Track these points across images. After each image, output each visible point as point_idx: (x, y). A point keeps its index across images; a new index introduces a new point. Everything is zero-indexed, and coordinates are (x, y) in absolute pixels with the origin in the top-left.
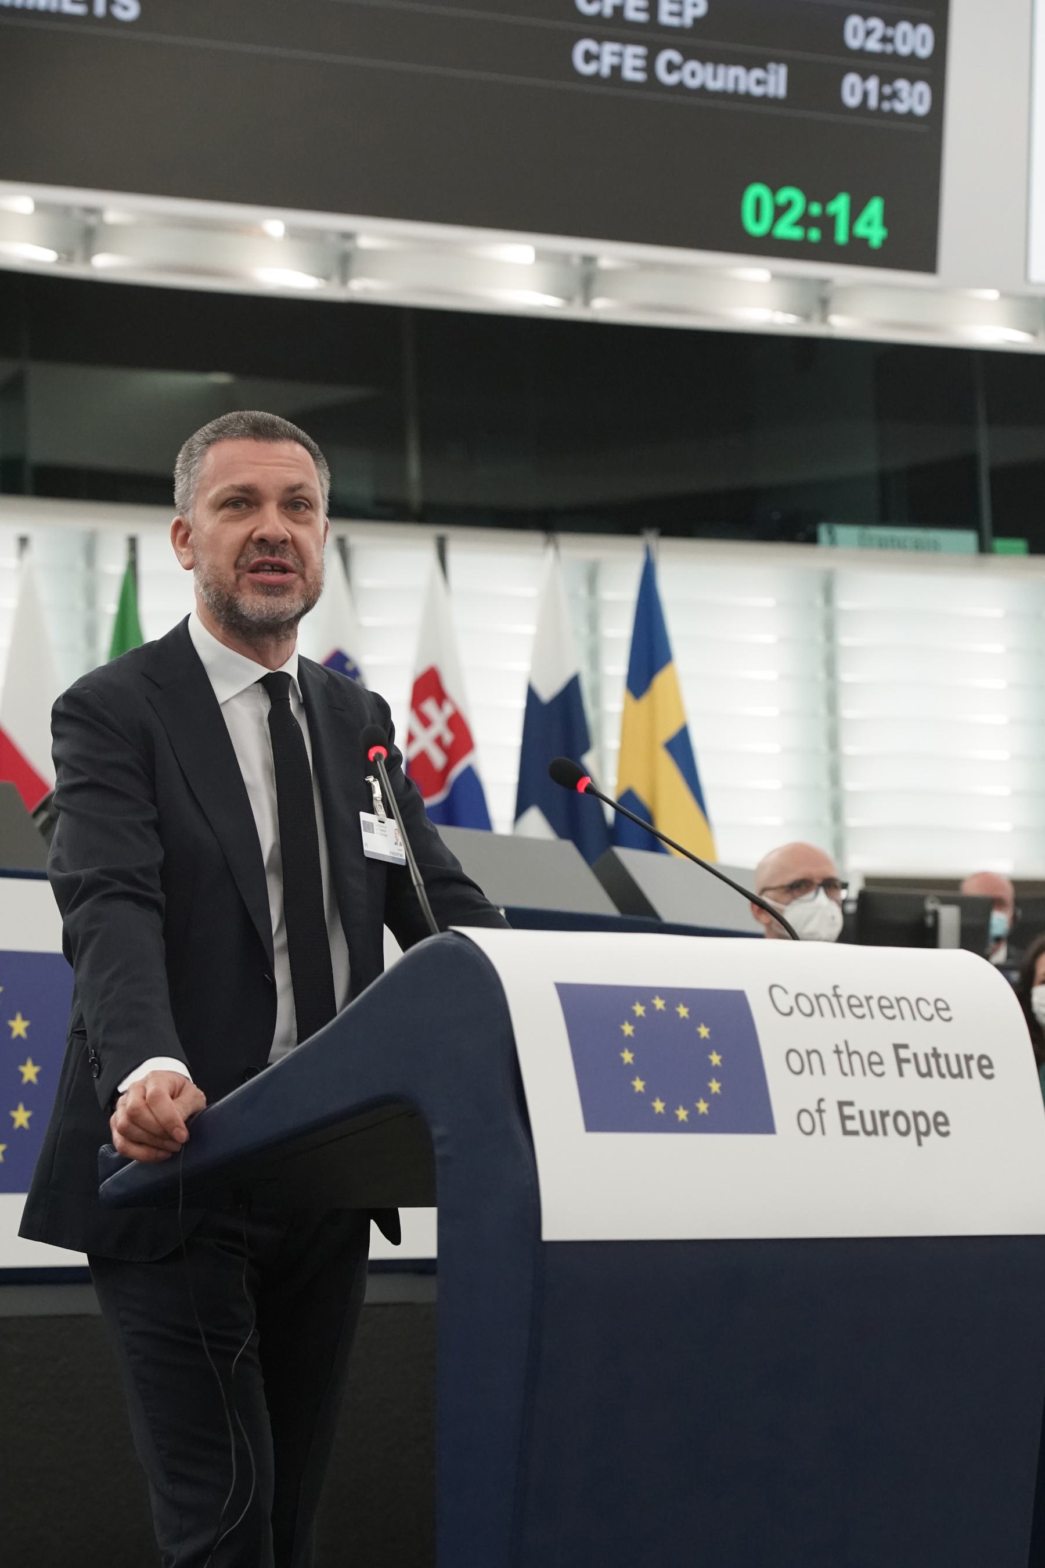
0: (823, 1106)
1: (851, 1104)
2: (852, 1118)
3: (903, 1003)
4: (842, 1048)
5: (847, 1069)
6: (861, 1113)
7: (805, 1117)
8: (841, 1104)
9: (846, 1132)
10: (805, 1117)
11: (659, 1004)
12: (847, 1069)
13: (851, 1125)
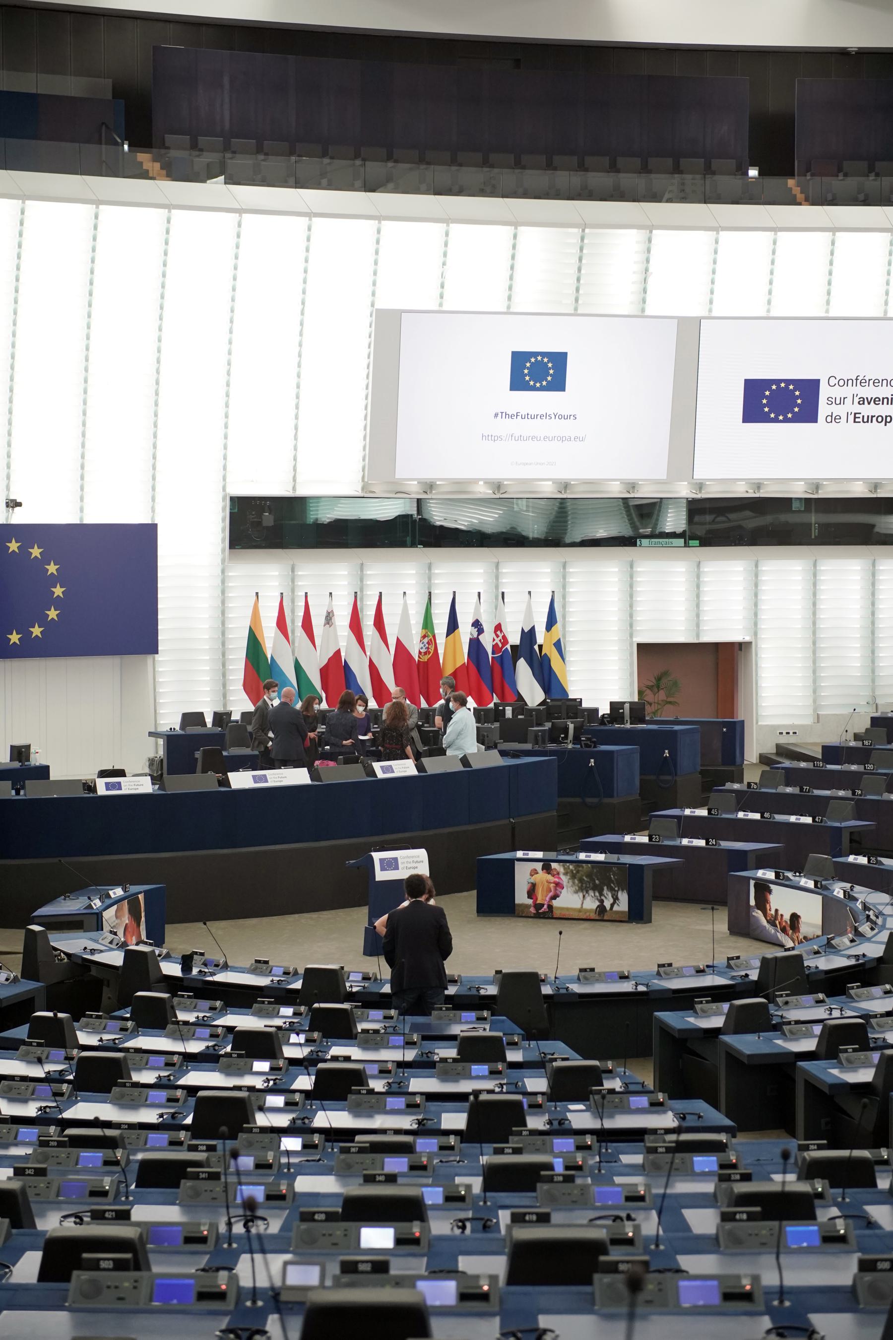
3: (885, 382)
9: (855, 422)
13: (857, 420)
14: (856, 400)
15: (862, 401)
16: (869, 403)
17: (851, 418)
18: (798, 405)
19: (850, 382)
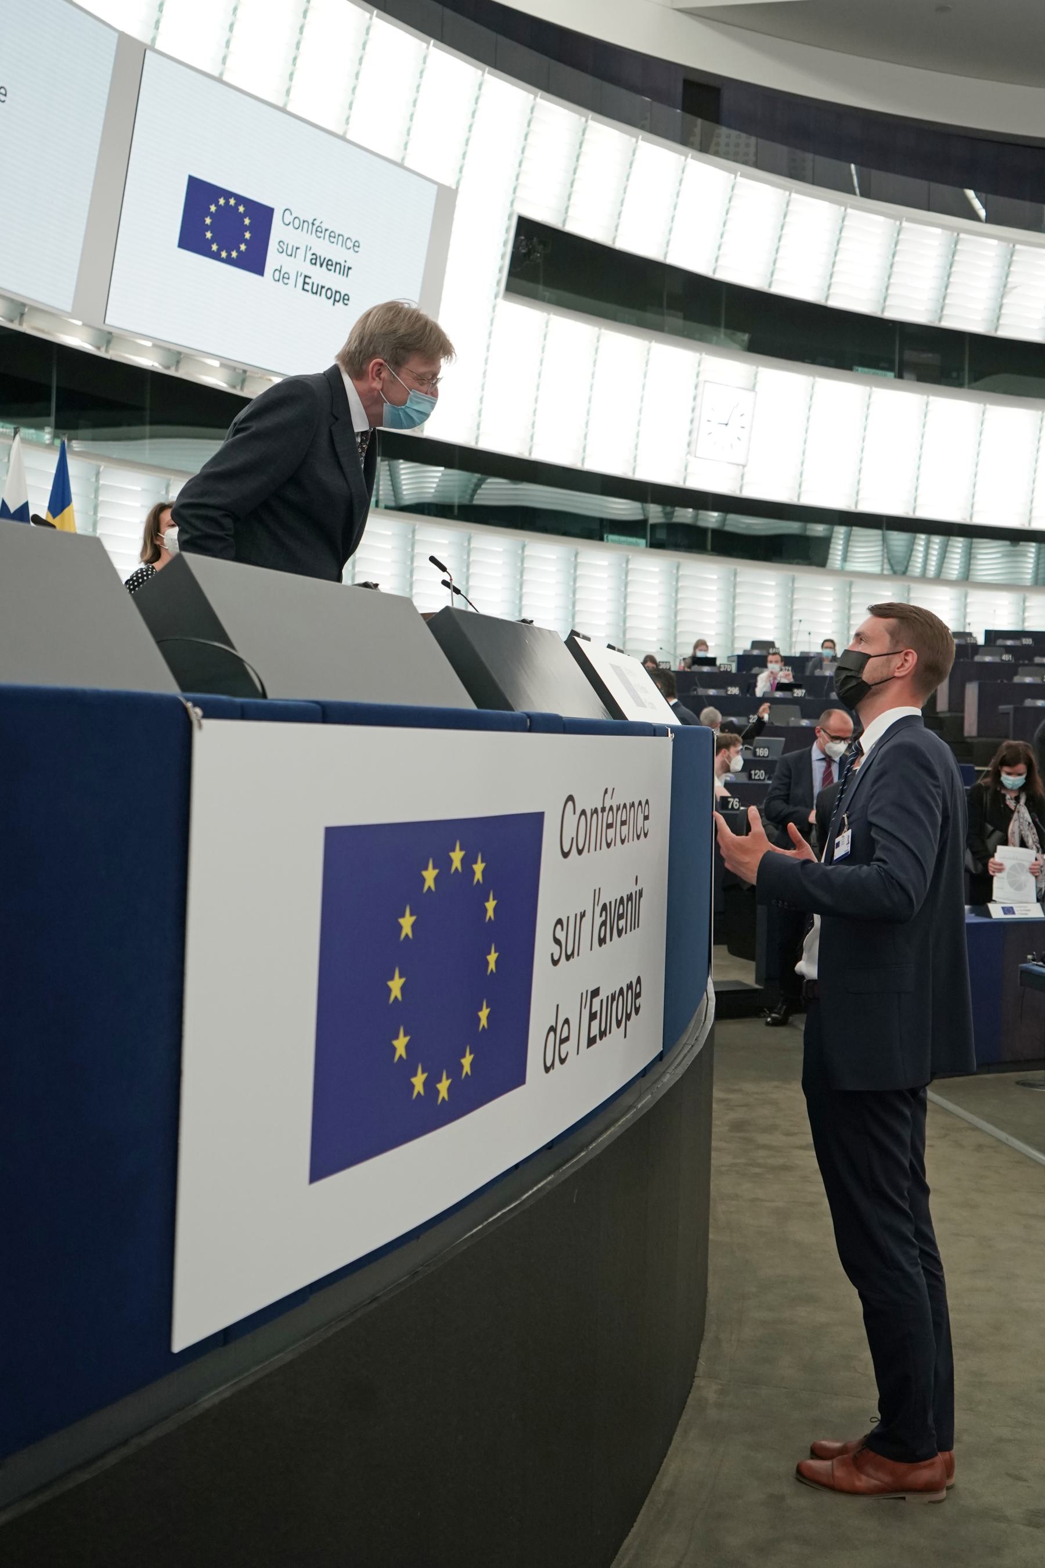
8: (306, 276)
11: (232, 202)
13: (306, 287)
14: (309, 256)
15: (315, 260)
16: (321, 265)
17: (301, 280)
18: (246, 242)
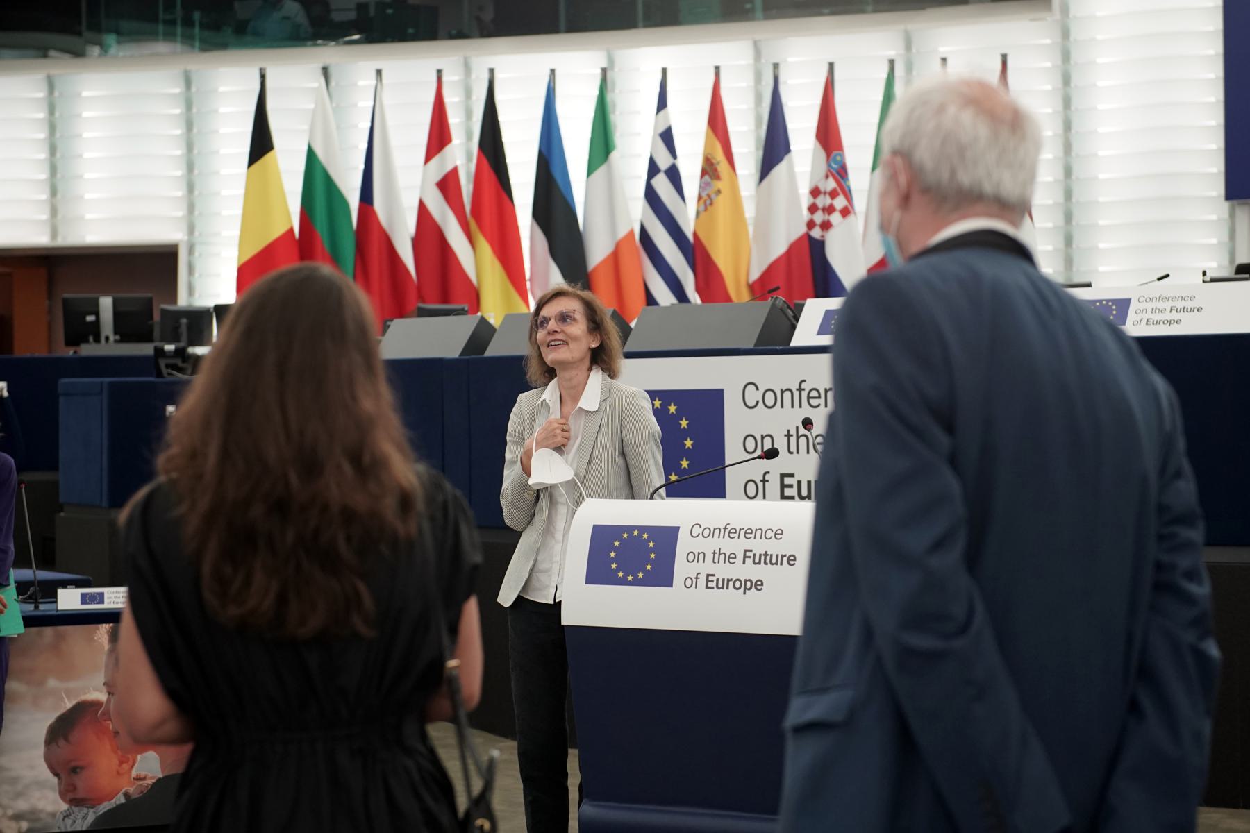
0: (767, 477)
1: (792, 475)
2: (791, 486)
4: (793, 432)
5: (793, 448)
6: (799, 483)
7: (751, 485)
8: (783, 476)
10: (751, 485)
12: (793, 448)
19: (787, 395)
